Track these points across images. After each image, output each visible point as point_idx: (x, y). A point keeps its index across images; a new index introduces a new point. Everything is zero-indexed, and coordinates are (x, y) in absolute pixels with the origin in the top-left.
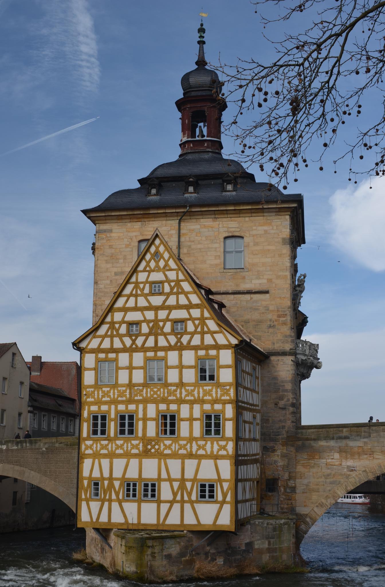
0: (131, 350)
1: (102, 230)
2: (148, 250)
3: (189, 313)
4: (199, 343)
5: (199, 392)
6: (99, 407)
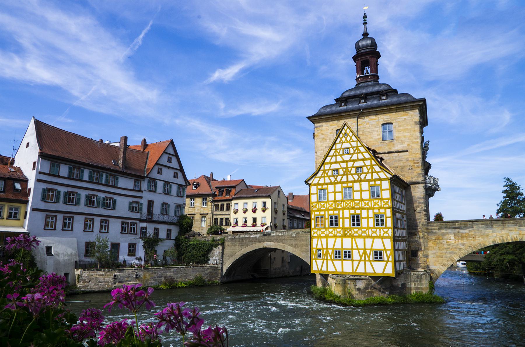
0: (335, 183)
2: (341, 132)
3: (364, 163)
4: (370, 178)
5: (371, 204)
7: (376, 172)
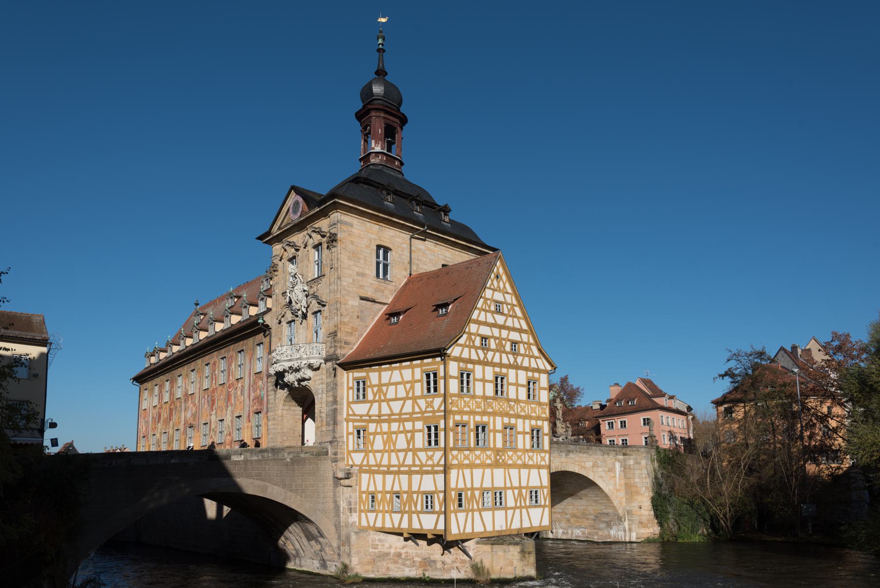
5: (528, 409)
7: (533, 356)
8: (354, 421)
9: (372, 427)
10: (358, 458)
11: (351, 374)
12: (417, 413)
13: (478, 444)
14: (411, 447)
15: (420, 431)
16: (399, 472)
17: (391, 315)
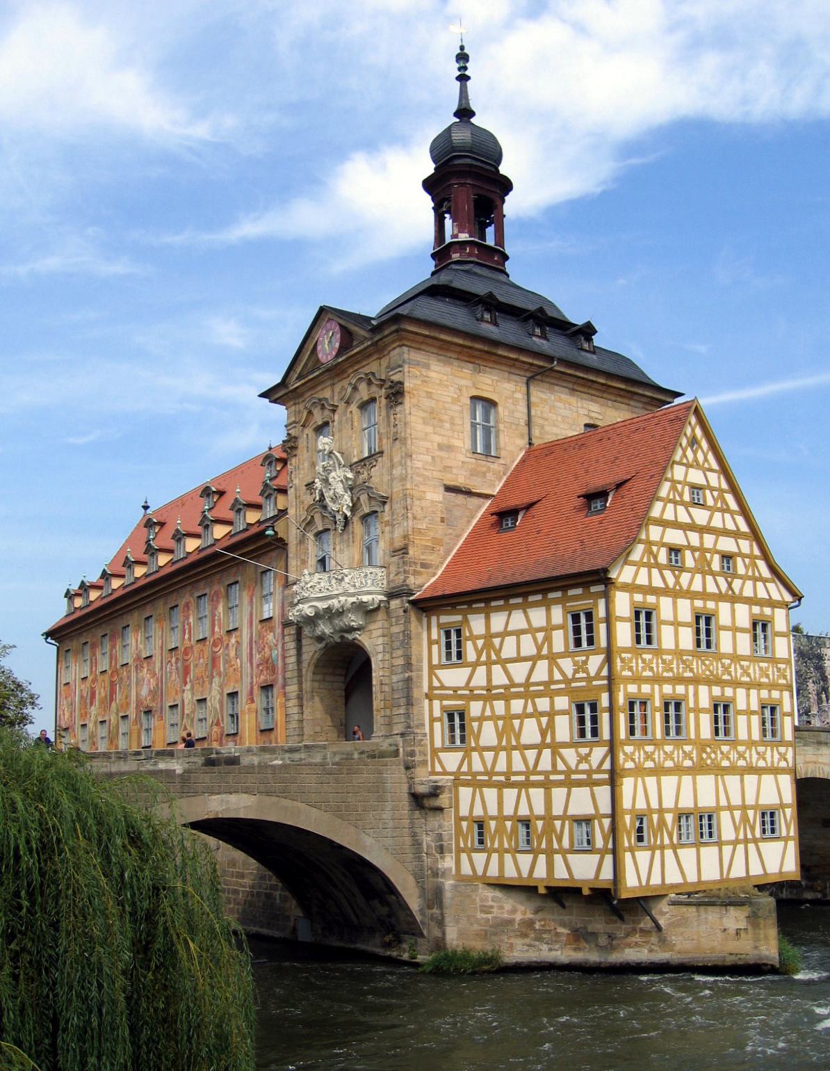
1: (414, 361)
6: (639, 688)
8: (442, 698)
9: (475, 708)
10: (451, 760)
11: (434, 619)
12: (558, 682)
13: (668, 734)
14: (548, 740)
15: (563, 712)
16: (527, 784)
17: (504, 516)
